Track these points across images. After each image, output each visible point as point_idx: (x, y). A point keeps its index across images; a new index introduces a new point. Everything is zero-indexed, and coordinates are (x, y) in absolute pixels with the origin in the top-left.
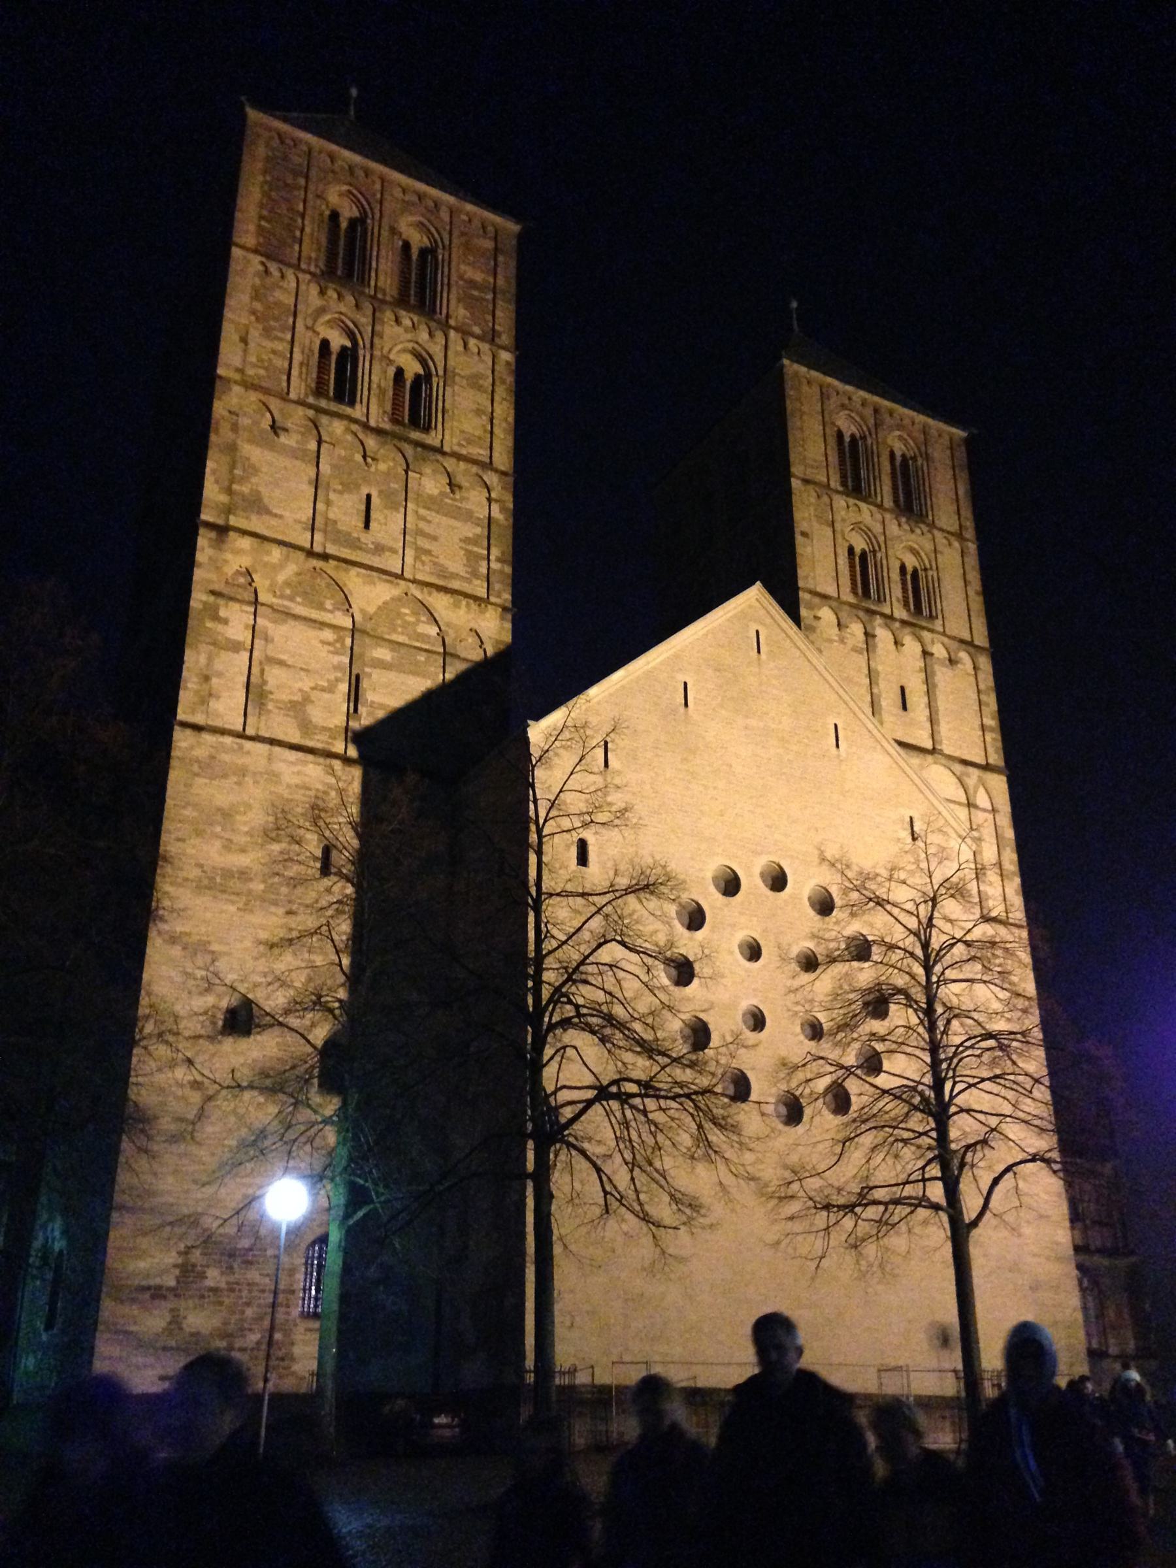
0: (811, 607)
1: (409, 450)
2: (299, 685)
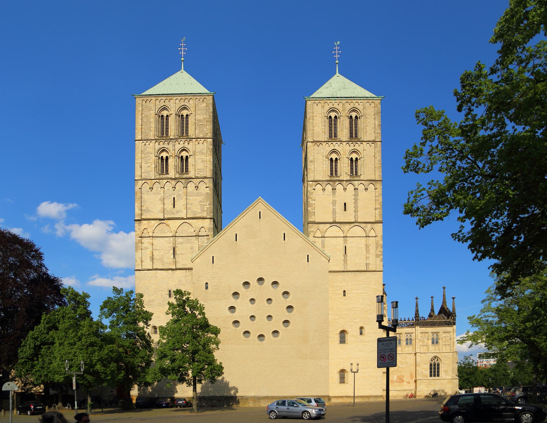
0: (311, 186)
1: (183, 181)
2: (161, 254)
